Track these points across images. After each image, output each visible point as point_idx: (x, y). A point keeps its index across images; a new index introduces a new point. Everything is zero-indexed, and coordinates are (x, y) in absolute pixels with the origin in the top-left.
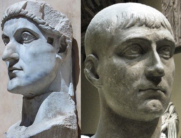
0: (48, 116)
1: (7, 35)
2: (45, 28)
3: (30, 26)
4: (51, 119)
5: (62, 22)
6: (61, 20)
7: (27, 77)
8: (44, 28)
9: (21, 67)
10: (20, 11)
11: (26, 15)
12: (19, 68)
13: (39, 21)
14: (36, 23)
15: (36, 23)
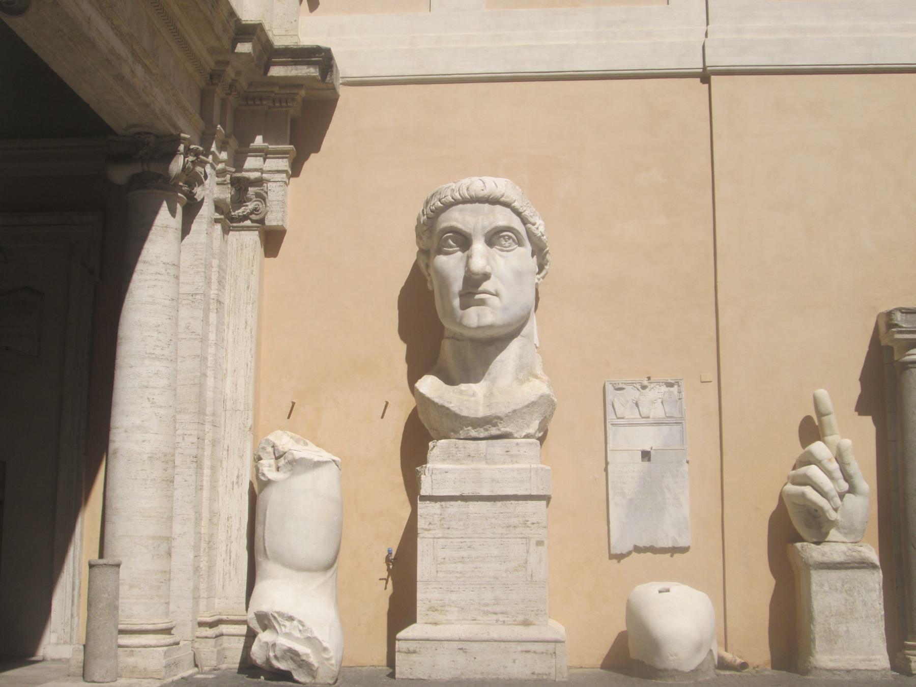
1: (468, 231)
3: (516, 223)
7: (505, 309)
14: (525, 221)
15: (525, 221)
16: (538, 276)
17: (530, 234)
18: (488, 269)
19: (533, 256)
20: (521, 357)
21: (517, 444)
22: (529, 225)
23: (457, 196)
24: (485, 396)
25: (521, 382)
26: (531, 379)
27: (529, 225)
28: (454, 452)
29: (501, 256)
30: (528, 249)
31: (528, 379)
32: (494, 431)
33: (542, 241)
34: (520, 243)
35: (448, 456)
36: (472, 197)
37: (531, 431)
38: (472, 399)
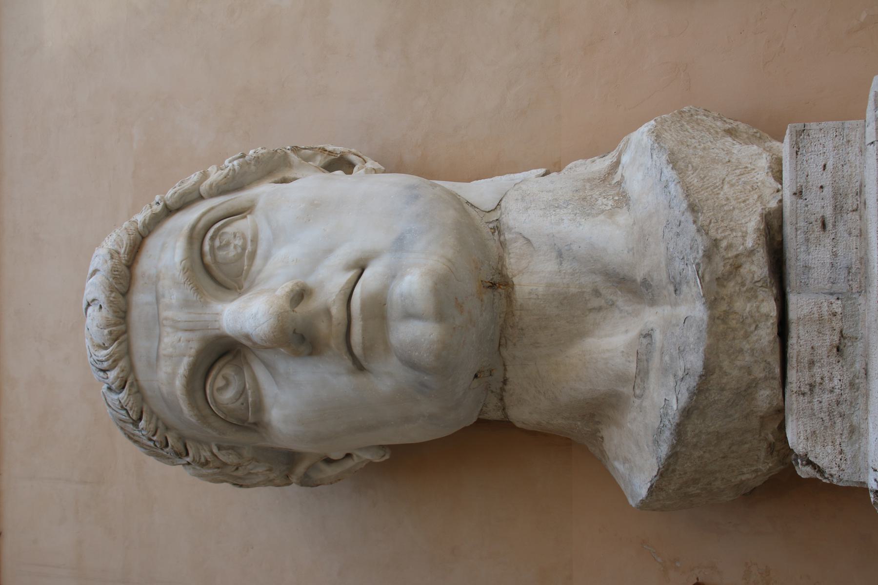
0: (608, 208)
1: (194, 347)
8: (228, 174)
9: (349, 268)
16: (355, 169)
17: (234, 184)
19: (295, 179)
20: (554, 205)
21: (799, 194)
22: (204, 188)
24: (653, 303)
25: (624, 200)
26: (617, 178)
27: (204, 188)
28: (826, 397)
29: (267, 258)
31: (619, 183)
32: (758, 268)
33: (257, 159)
36: (115, 338)
37: (763, 162)
38: (658, 336)
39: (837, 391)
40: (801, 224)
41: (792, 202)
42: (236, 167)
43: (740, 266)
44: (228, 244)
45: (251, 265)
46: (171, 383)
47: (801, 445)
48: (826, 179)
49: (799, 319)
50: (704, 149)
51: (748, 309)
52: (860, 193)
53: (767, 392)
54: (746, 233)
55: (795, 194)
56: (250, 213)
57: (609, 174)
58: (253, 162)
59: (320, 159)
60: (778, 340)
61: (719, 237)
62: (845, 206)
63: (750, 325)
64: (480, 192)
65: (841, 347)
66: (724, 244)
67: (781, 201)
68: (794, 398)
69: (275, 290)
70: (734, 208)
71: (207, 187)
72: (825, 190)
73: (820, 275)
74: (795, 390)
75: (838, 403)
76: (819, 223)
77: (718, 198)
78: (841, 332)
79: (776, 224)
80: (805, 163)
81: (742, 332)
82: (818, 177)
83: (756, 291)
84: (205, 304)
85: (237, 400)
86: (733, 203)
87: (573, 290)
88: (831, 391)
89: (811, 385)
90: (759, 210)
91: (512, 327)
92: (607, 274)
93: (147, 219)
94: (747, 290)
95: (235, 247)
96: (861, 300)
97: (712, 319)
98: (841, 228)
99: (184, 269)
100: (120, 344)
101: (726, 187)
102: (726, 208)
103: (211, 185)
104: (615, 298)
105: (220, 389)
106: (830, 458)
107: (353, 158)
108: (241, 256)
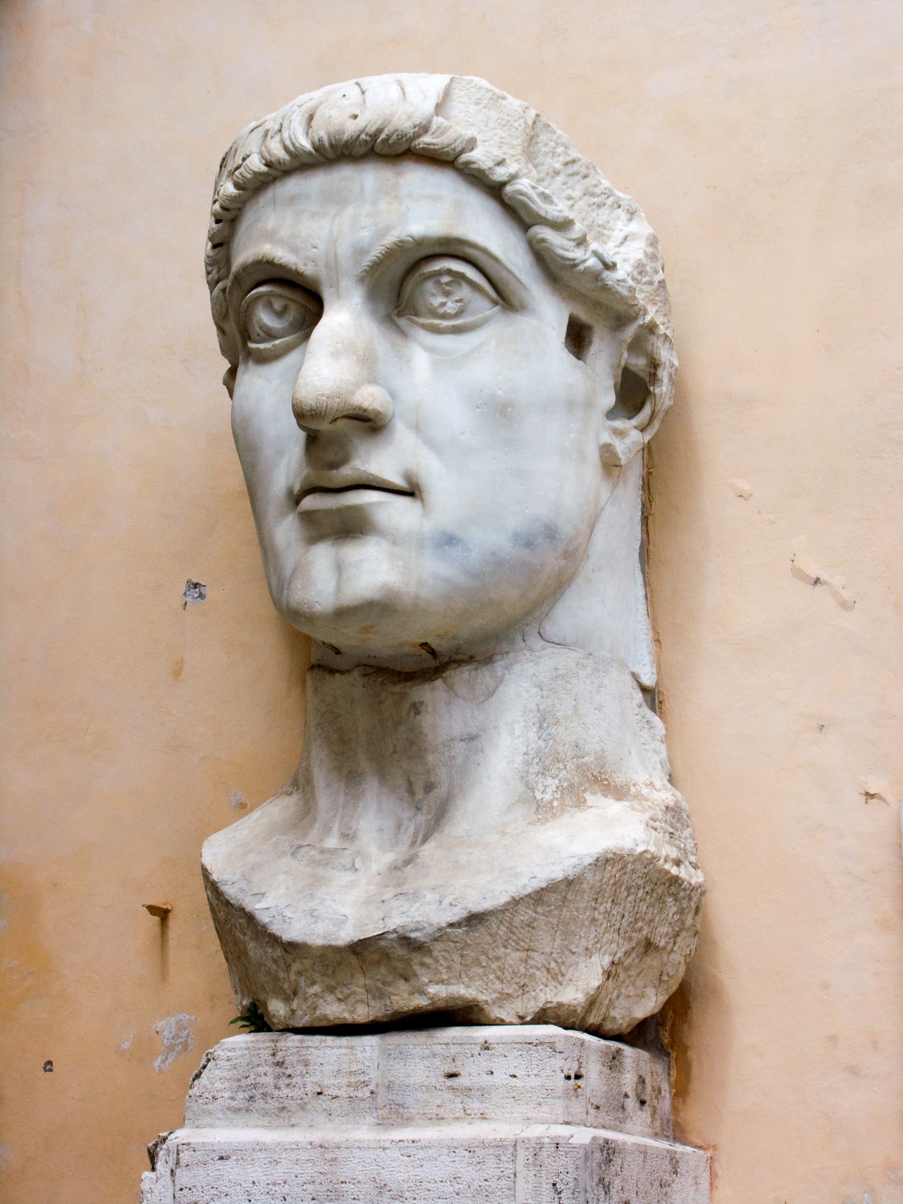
0: (539, 796)
1: (307, 269)
2: (571, 255)
3: (485, 229)
4: (554, 816)
5: (626, 238)
6: (620, 225)
8: (563, 258)
10: (424, 129)
11: (464, 158)
12: (399, 481)
13: (539, 208)
14: (517, 213)
15: (517, 213)
17: (552, 269)
18: (369, 397)
23: (278, 152)
28: (269, 1080)
29: (430, 350)
30: (549, 315)
32: (406, 999)
34: (505, 299)
35: (252, 1100)
37: (572, 995)
39: (276, 1093)
40: (454, 1050)
41: (477, 1038)
42: (581, 267)
43: (406, 980)
44: (447, 294)
45: (424, 327)
46: (271, 236)
47: (222, 1054)
48: (500, 1078)
49: (352, 1048)
50: (594, 920)
51: (357, 989)
52: (483, 1117)
53: (282, 1012)
54: (449, 984)
55: (486, 1042)
56: (503, 307)
57: (609, 784)
58: (600, 283)
59: (639, 363)
60: (332, 1024)
61: (434, 954)
62: (470, 1100)
63: (341, 992)
64: (607, 603)
65: (321, 1096)
66: (428, 960)
67: (501, 1022)
68: (269, 1044)
69: (373, 380)
70: (484, 967)
71: (540, 236)
72: (489, 1077)
73: (401, 1072)
74: (278, 1044)
75: (265, 1095)
76: (453, 1070)
77: (497, 946)
78: (337, 1097)
79: (474, 1017)
80: (520, 1053)
81: (333, 983)
82: (502, 1068)
83: (381, 998)
84: (361, 280)
85: (261, 328)
86: (494, 965)
87: (431, 758)
88: (276, 1087)
89: (283, 1063)
90: (482, 997)
91: (382, 683)
92: (447, 801)
93: (475, 166)
94: (379, 988)
95: (443, 304)
96: (370, 1119)
97: (337, 950)
98: (448, 1095)
99: (401, 241)
100: (310, 153)
101: (523, 955)
102: (483, 958)
103: (543, 240)
104: (424, 811)
105: (269, 306)
106: (209, 1086)
107: (647, 410)
108: (435, 314)
